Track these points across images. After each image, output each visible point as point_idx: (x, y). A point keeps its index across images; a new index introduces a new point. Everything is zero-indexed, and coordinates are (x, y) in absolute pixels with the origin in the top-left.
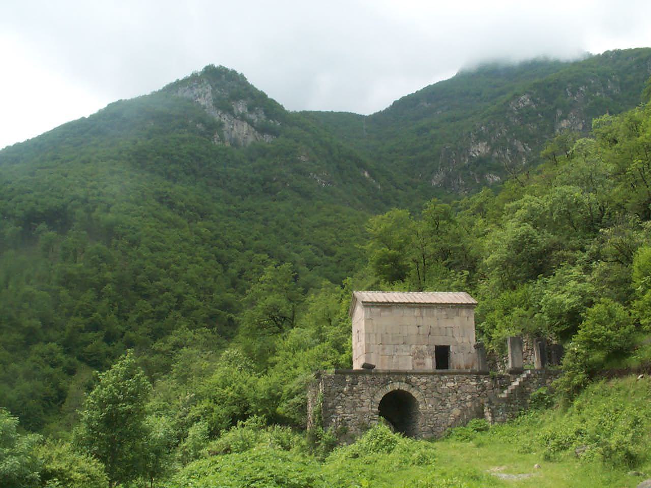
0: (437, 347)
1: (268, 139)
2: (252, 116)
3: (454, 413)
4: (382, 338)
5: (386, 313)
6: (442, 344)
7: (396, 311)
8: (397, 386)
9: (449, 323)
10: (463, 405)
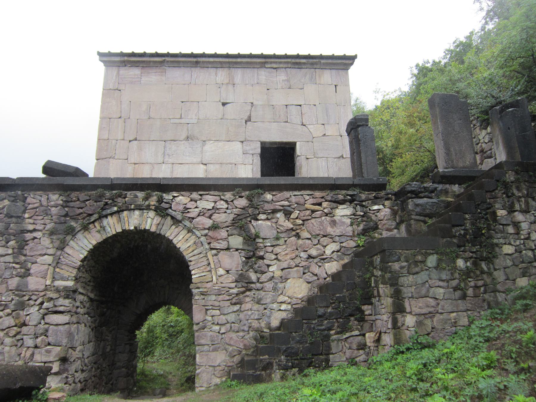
0: (263, 144)
3: (290, 293)
6: (278, 140)
8: (133, 221)
9: (294, 98)
10: (315, 269)
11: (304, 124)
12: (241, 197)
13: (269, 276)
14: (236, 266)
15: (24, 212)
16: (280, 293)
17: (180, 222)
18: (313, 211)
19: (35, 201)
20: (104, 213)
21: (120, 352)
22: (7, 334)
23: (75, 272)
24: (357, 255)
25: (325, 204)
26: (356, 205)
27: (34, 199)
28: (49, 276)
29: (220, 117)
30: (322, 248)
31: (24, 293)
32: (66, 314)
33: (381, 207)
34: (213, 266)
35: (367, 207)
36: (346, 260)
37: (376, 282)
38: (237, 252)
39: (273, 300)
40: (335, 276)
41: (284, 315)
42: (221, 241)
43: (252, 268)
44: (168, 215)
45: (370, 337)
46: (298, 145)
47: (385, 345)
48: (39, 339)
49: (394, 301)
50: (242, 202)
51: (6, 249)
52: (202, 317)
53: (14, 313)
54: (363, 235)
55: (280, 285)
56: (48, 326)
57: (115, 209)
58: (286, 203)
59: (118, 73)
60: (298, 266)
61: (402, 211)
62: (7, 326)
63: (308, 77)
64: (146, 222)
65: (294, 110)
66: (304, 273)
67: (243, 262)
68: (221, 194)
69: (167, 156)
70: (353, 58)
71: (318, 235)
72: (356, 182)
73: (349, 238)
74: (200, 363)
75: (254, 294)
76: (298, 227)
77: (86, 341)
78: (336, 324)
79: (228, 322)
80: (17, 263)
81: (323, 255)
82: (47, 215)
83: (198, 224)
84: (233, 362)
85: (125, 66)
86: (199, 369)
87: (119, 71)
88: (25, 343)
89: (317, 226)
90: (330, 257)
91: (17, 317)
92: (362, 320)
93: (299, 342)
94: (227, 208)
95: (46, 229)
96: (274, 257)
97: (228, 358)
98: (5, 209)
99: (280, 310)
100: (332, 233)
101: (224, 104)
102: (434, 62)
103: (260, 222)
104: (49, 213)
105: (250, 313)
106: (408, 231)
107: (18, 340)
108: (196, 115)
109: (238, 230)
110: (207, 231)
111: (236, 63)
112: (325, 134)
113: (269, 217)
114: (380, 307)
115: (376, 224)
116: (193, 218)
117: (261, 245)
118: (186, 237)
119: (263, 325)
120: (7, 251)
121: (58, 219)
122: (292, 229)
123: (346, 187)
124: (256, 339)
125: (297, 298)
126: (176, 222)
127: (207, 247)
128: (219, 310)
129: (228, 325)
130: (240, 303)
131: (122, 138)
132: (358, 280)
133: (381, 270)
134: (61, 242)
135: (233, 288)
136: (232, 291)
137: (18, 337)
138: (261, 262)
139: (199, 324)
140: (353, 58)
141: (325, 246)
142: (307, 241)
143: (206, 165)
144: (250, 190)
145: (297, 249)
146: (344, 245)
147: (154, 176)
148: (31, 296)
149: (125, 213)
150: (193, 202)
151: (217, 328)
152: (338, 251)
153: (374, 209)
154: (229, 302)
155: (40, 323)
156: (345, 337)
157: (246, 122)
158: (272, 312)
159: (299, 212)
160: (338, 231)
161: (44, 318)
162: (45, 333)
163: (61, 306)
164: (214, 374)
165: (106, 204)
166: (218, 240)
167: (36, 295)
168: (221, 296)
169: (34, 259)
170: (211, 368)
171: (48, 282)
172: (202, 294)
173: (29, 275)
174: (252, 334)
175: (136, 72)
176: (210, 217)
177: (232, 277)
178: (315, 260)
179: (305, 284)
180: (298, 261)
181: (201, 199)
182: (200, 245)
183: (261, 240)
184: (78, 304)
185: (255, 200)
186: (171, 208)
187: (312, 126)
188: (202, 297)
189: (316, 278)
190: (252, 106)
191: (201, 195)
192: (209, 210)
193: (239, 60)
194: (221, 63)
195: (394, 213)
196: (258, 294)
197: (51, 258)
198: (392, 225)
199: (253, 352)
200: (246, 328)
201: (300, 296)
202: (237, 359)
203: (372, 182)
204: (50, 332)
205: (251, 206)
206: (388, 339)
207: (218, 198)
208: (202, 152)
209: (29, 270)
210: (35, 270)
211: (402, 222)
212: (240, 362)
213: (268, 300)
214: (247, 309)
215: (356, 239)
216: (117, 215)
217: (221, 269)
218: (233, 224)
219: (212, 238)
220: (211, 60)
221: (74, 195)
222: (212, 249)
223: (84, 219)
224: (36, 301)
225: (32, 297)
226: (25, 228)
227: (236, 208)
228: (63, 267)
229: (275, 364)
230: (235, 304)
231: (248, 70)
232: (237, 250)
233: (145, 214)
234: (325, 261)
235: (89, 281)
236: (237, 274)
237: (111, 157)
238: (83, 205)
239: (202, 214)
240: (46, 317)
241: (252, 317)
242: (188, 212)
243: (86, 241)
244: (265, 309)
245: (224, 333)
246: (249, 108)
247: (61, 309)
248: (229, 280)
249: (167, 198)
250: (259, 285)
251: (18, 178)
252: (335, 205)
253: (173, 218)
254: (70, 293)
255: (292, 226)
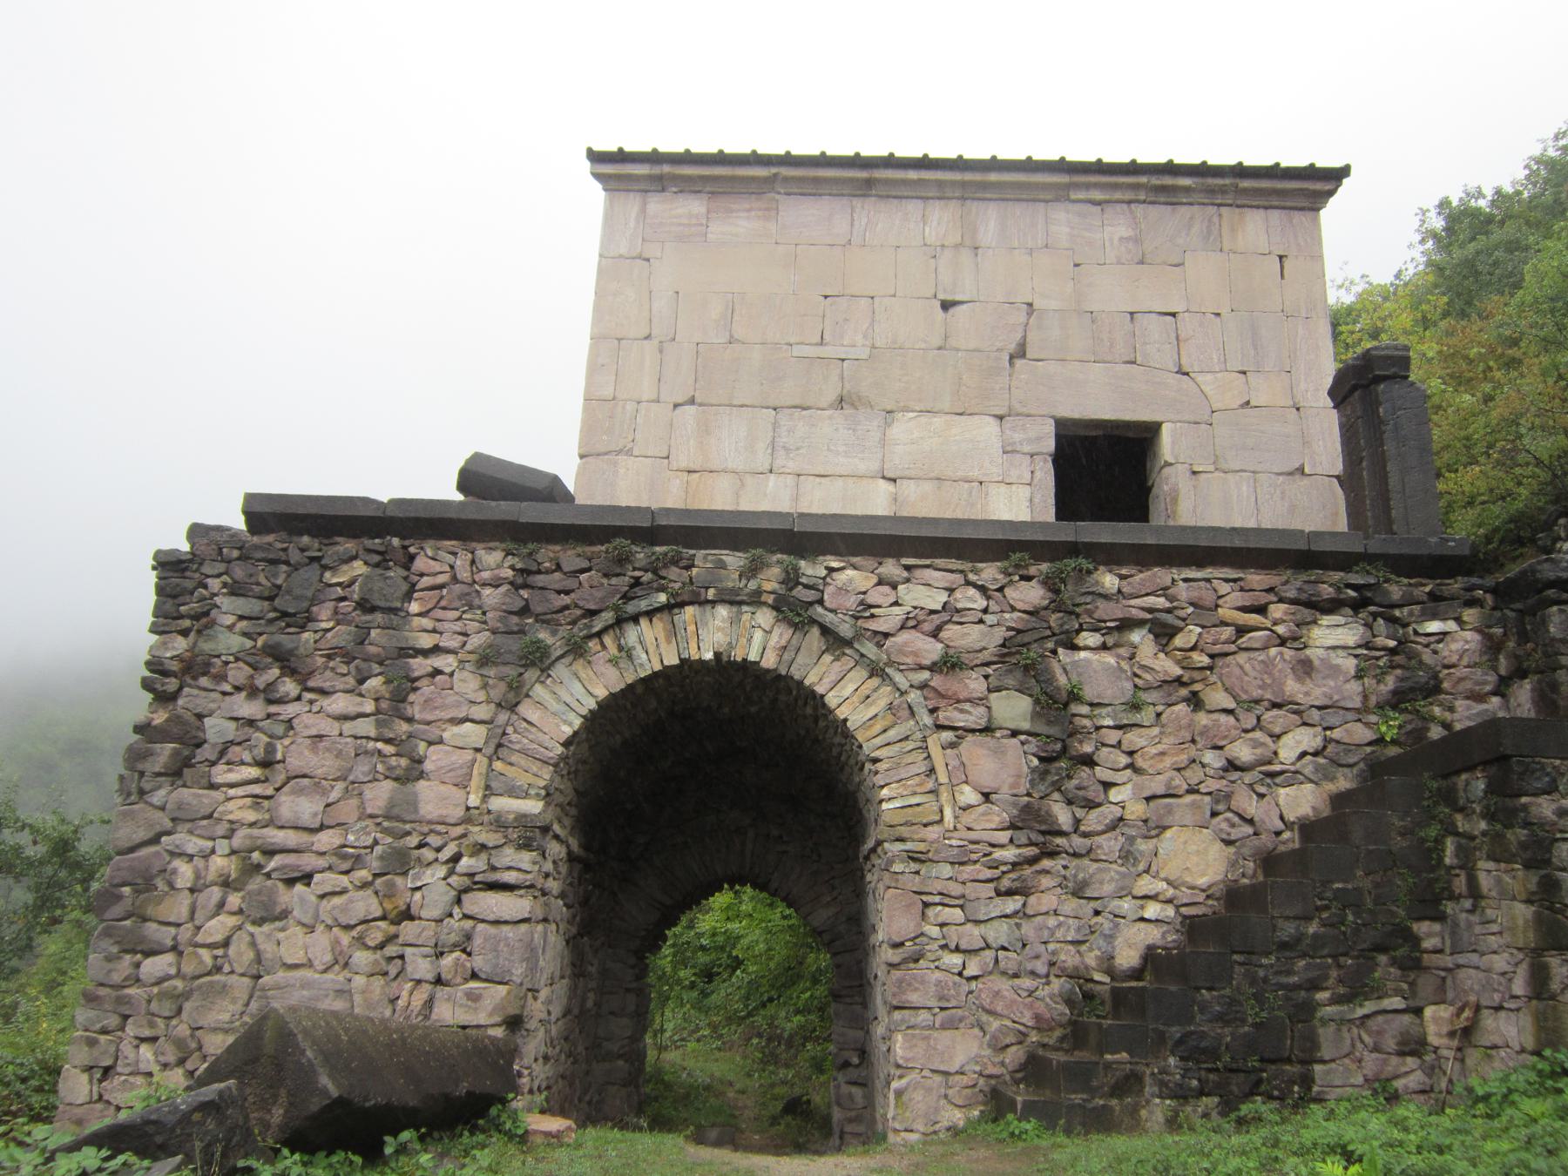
3: (1171, 870)
5: (739, 224)
8: (711, 634)
10: (1251, 807)
11: (1185, 369)
12: (1028, 578)
13: (1111, 817)
14: (1011, 780)
15: (408, 596)
16: (1141, 867)
17: (848, 643)
18: (1242, 630)
19: (437, 567)
20: (631, 608)
21: (612, 1013)
22: (360, 942)
23: (547, 772)
24: (1376, 770)
25: (1277, 611)
26: (1375, 616)
27: (433, 561)
28: (476, 782)
29: (937, 342)
30: (1269, 740)
31: (408, 827)
32: (522, 892)
33: (1451, 626)
34: (943, 778)
35: (1405, 625)
36: (1344, 782)
37: (1460, 851)
38: (1014, 741)
39: (1122, 889)
40: (1307, 828)
41: (1153, 935)
42: (967, 706)
43: (1059, 790)
44: (813, 621)
45: (1437, 1020)
46: (1166, 430)
47: (1495, 1047)
48: (448, 961)
49: (1538, 915)
50: (1030, 594)
51: (359, 699)
52: (912, 925)
53: (379, 881)
54: (1394, 707)
55: (1143, 846)
56: (470, 923)
57: (662, 598)
58: (1161, 602)
59: (643, 210)
60: (1197, 792)
61: (1523, 637)
62: (361, 916)
63: (1195, 229)
64: (750, 640)
65: (1155, 328)
66: (1214, 814)
67: (1033, 770)
68: (967, 566)
69: (782, 452)
70: (1337, 175)
71: (1257, 702)
72: (1375, 547)
73: (1350, 716)
74: (908, 1060)
75: (1065, 867)
76: (1197, 675)
77: (558, 974)
78: (1334, 973)
79: (988, 947)
80: (388, 741)
81: (1270, 763)
82: (471, 607)
83: (901, 652)
84: (1002, 1064)
85: (663, 190)
86: (901, 1077)
87: (645, 204)
88: (409, 969)
89: (1253, 674)
90: (1292, 768)
91: (390, 893)
92: (1412, 964)
93: (1221, 1018)
94: (985, 611)
95: (468, 647)
96: (1124, 760)
97: (987, 1052)
98: (356, 587)
99: (1142, 919)
100: (1300, 698)
101: (946, 306)
102: (1498, 192)
103: (1083, 654)
104: (476, 602)
105: (1052, 922)
106: (1546, 697)
107: (390, 959)
108: (865, 337)
109: (1019, 674)
110: (926, 675)
111: (985, 186)
112: (1248, 403)
113: (1110, 641)
114: (1478, 929)
115: (1435, 676)
116: (886, 635)
117: (1086, 722)
118: (865, 690)
119: (1091, 959)
120: (361, 704)
121: (501, 619)
122: (1178, 681)
123: (1344, 561)
124: (1069, 1002)
125: (1193, 888)
126: (835, 642)
127: (927, 720)
128: (961, 907)
129: (989, 954)
130: (1022, 891)
131: (654, 397)
132: (1399, 843)
133: (1489, 816)
134: (510, 687)
135: (1002, 846)
136: (998, 854)
137: (391, 950)
138: (1084, 772)
139: (902, 944)
140: (1337, 175)
141: (1279, 737)
142: (1223, 718)
143: (894, 481)
144: (1052, 561)
145: (1193, 741)
146: (1336, 734)
147: (746, 506)
148: (426, 835)
149: (690, 610)
150: (886, 589)
151: (955, 960)
152: (1315, 754)
153: (1429, 630)
154: (991, 885)
155: (451, 915)
156: (1360, 1012)
157: (1012, 357)
158: (1117, 925)
159: (1199, 630)
160: (1318, 692)
161: (459, 901)
162: (464, 945)
163: (509, 868)
164: (946, 1096)
165: (637, 582)
166: (958, 701)
167: (439, 833)
168: (969, 868)
169: (433, 732)
170: (938, 1078)
171: (474, 800)
172: (913, 857)
173: (422, 775)
174: (1057, 984)
175: (693, 206)
176: (935, 634)
177: (1000, 814)
178: (1248, 778)
179: (1219, 845)
180: (1194, 775)
181: (908, 580)
182: (907, 712)
183: (1085, 710)
184: (548, 866)
185: (1068, 591)
186: (821, 602)
187: (1209, 377)
188: (914, 866)
189: (1249, 830)
190: (1030, 314)
191: (908, 568)
192: (933, 612)
193: (993, 177)
194: (940, 184)
195: (1493, 647)
196: (1078, 868)
197: (481, 731)
198: (1485, 683)
199: (1062, 1039)
200: (1041, 968)
201: (1202, 881)
202: (1014, 1056)
203: (1424, 551)
204: (478, 941)
205: (1057, 605)
206: (1510, 1029)
207: (959, 578)
208: (883, 442)
209: (420, 762)
210: (440, 764)
211: (1520, 673)
212: (1023, 1067)
213: (1108, 888)
214: (1044, 909)
215: (1373, 718)
216: (666, 616)
217: (967, 788)
218: (1002, 658)
219: (943, 696)
220: (912, 175)
221: (546, 554)
222: (940, 727)
223: (574, 623)
224: (438, 850)
225: (429, 839)
226: (411, 643)
227: (1013, 609)
228: (514, 758)
229: (1148, 1080)
230: (1010, 893)
231: (1018, 209)
232: (1015, 733)
233: (746, 617)
234: (1278, 780)
235: (569, 804)
236: (1015, 805)
237: (619, 452)
238: (570, 583)
239: (911, 623)
240: (464, 897)
241: (1059, 935)
242: (873, 616)
243: (577, 687)
244: (1097, 913)
245: (975, 978)
246: (1022, 318)
247: (510, 877)
248: (990, 822)
249: (810, 572)
250: (1078, 842)
251: (392, 501)
252: (1306, 613)
253: (826, 631)
254: (529, 834)
255: (1178, 671)
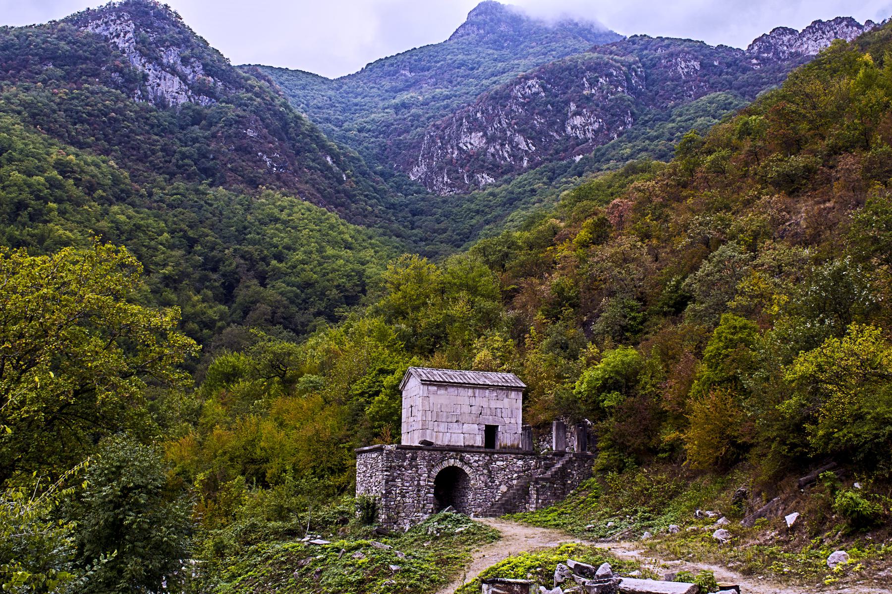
1: (205, 100)
2: (187, 70)
4: (437, 416)
5: (442, 392)
7: (451, 390)
9: (499, 404)
50: (488, 458)
